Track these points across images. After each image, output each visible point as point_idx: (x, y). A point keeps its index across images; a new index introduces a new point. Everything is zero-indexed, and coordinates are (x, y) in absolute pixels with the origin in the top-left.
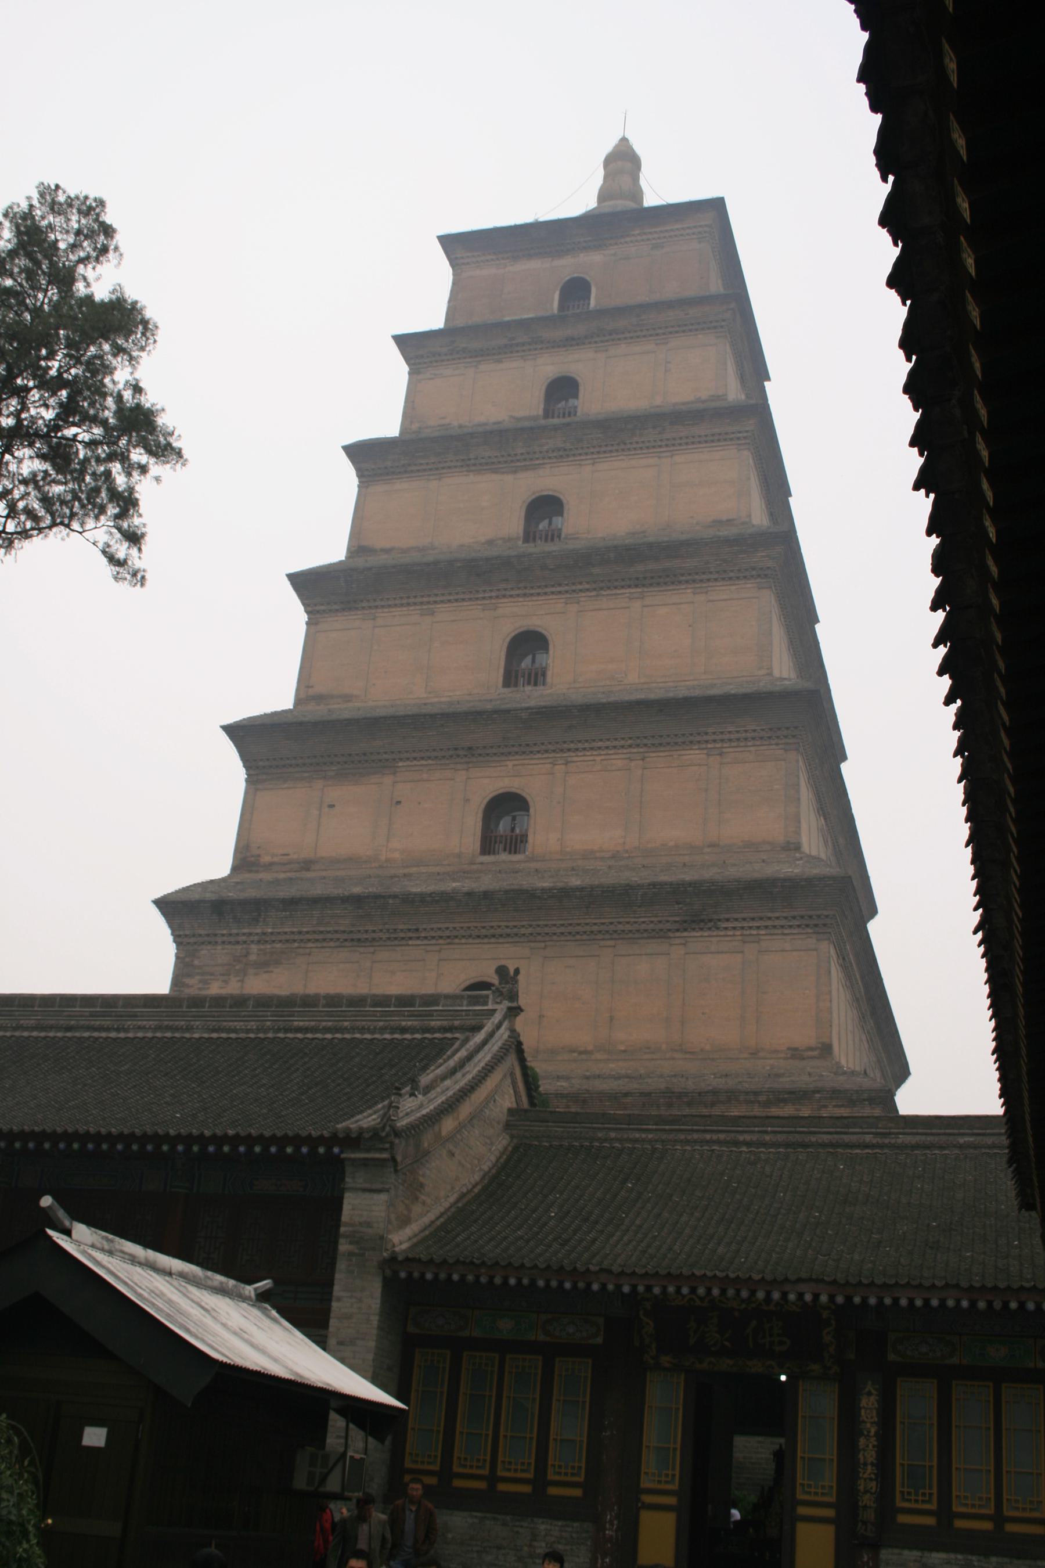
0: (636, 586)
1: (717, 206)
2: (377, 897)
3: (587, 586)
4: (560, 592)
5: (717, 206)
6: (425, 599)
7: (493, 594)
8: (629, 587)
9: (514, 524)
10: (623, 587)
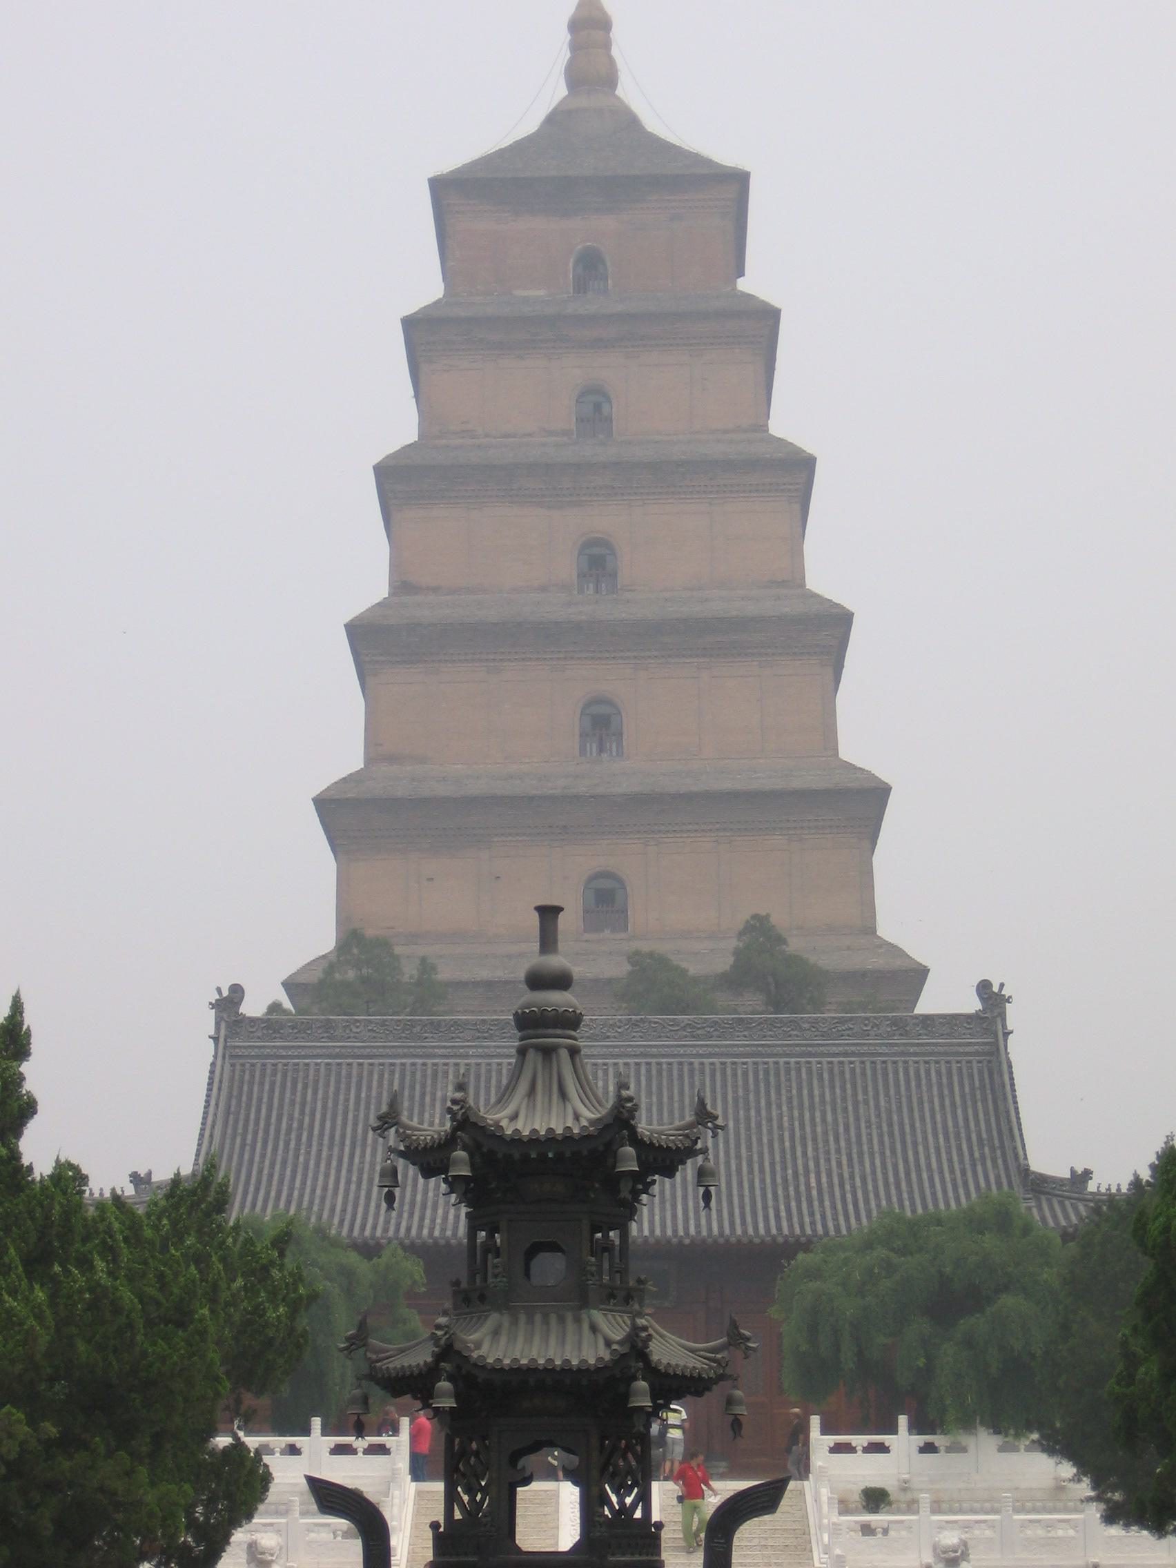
0: (704, 656)
1: (740, 180)
2: (507, 982)
3: (655, 653)
4: (628, 658)
5: (740, 180)
6: (492, 657)
7: (562, 656)
8: (697, 656)
9: (566, 567)
10: (691, 656)
